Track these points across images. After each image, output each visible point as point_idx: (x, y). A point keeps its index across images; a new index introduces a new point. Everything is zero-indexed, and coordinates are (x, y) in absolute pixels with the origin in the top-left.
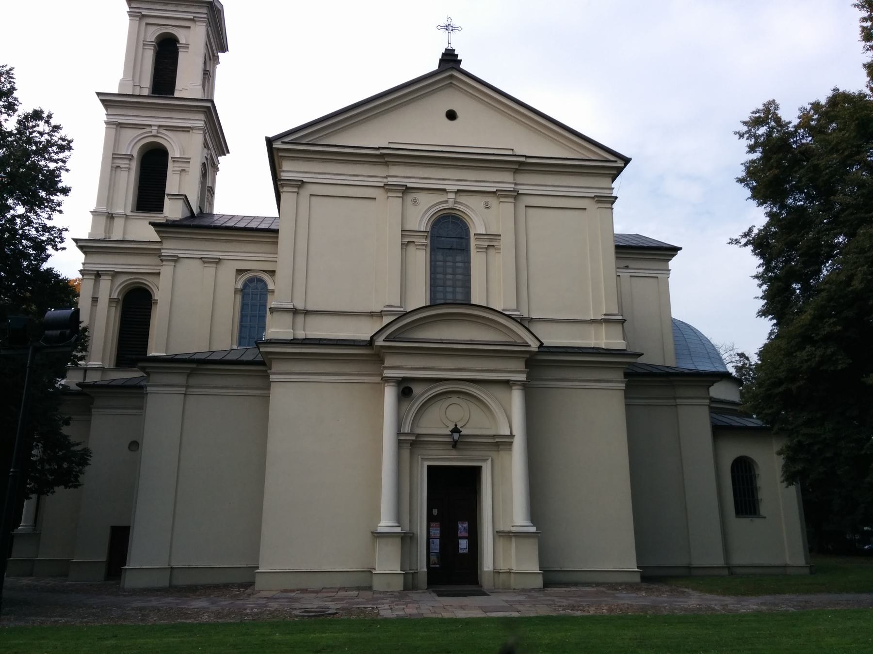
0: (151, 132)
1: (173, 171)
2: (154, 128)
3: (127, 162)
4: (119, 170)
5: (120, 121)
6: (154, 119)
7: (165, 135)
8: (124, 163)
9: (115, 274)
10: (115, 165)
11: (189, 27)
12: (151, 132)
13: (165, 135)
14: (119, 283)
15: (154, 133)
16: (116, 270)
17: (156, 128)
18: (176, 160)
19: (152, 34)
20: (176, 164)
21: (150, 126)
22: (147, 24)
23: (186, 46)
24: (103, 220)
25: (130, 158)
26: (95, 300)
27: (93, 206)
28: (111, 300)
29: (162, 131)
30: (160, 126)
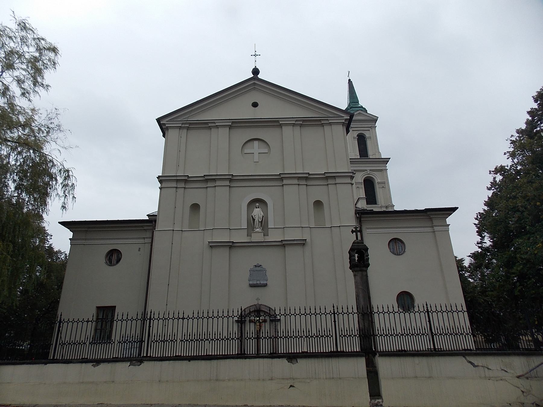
2: (368, 171)
4: (358, 188)
5: (355, 169)
6: (368, 167)
7: (372, 173)
8: (359, 186)
10: (357, 187)
11: (369, 130)
12: (367, 173)
13: (372, 173)
15: (369, 173)
18: (379, 183)
20: (379, 185)
21: (366, 170)
22: (353, 130)
25: (360, 183)
30: (370, 170)
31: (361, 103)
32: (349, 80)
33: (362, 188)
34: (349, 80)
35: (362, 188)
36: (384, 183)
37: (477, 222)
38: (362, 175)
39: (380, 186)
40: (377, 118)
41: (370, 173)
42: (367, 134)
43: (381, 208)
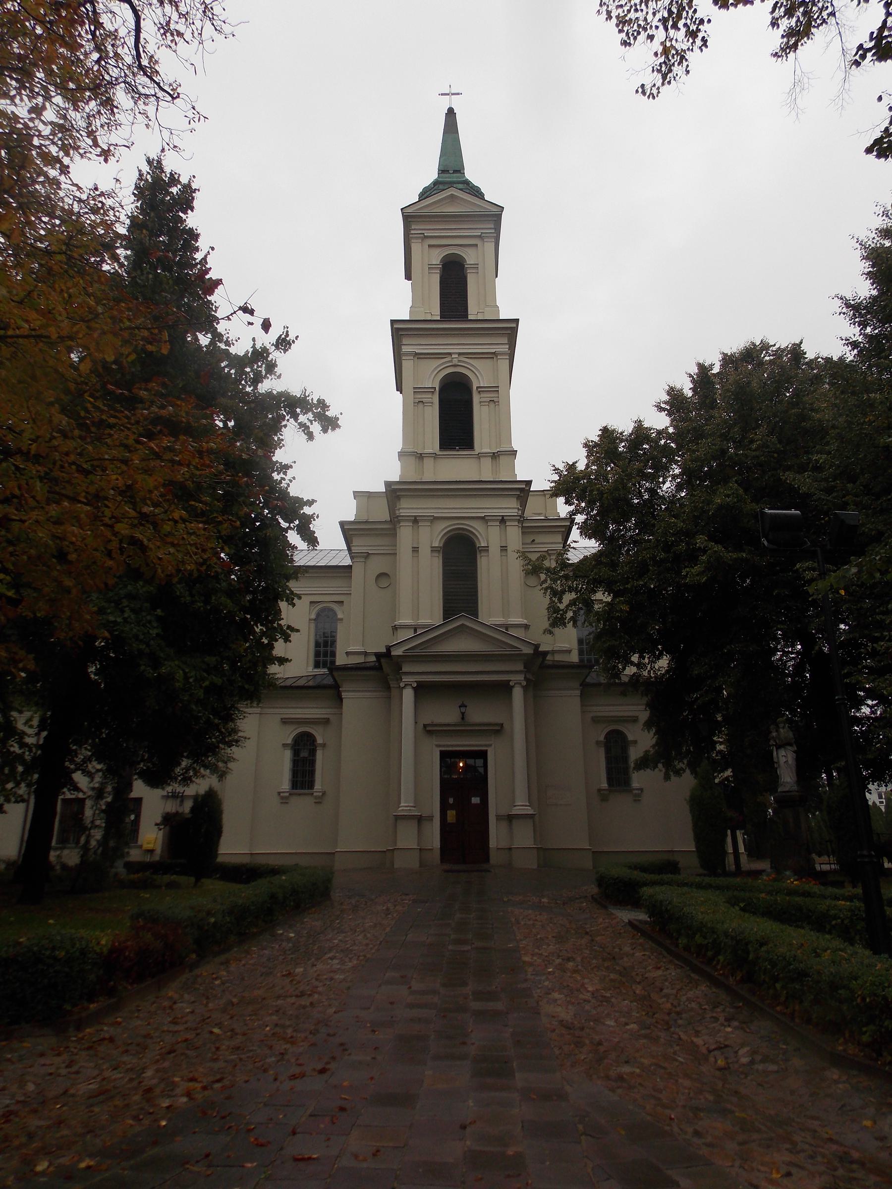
0: (451, 361)
1: (480, 402)
3: (430, 396)
4: (421, 405)
6: (454, 347)
8: (426, 397)
9: (435, 519)
10: (417, 400)
11: (476, 245)
14: (440, 530)
15: (455, 362)
16: (435, 515)
17: (457, 356)
19: (436, 257)
20: (483, 395)
21: (450, 354)
22: (430, 246)
23: (476, 267)
24: (412, 460)
26: (415, 550)
27: (398, 446)
28: (434, 550)
29: (462, 358)
30: (460, 354)
31: (471, 174)
32: (451, 113)
33: (432, 403)
34: (451, 113)
35: (432, 403)
36: (495, 390)
37: (145, 168)
38: (436, 368)
39: (483, 399)
40: (500, 209)
41: (459, 361)
42: (470, 257)
43: (479, 458)
